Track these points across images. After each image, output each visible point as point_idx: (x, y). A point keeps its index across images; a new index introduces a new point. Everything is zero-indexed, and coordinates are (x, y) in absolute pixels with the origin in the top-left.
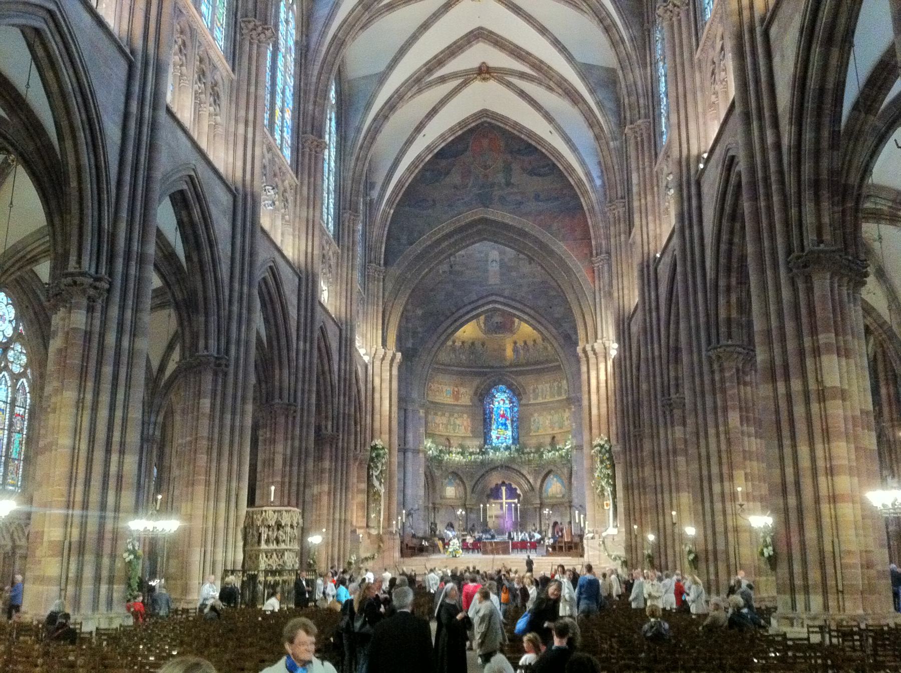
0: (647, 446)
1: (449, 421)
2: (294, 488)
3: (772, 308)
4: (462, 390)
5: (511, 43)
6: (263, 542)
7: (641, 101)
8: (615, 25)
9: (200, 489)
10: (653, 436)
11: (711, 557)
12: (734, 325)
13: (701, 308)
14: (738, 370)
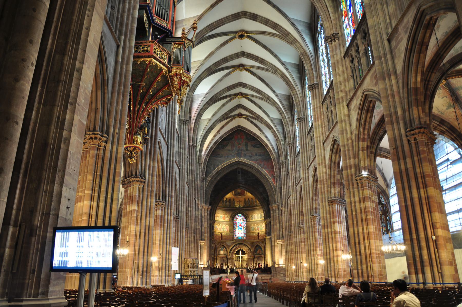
0: (293, 240)
1: (221, 227)
2: (188, 252)
3: (324, 211)
4: (226, 216)
6: (189, 268)
7: (291, 136)
8: (283, 113)
10: (295, 237)
11: (311, 271)
12: (317, 209)
13: (309, 204)
14: (318, 221)
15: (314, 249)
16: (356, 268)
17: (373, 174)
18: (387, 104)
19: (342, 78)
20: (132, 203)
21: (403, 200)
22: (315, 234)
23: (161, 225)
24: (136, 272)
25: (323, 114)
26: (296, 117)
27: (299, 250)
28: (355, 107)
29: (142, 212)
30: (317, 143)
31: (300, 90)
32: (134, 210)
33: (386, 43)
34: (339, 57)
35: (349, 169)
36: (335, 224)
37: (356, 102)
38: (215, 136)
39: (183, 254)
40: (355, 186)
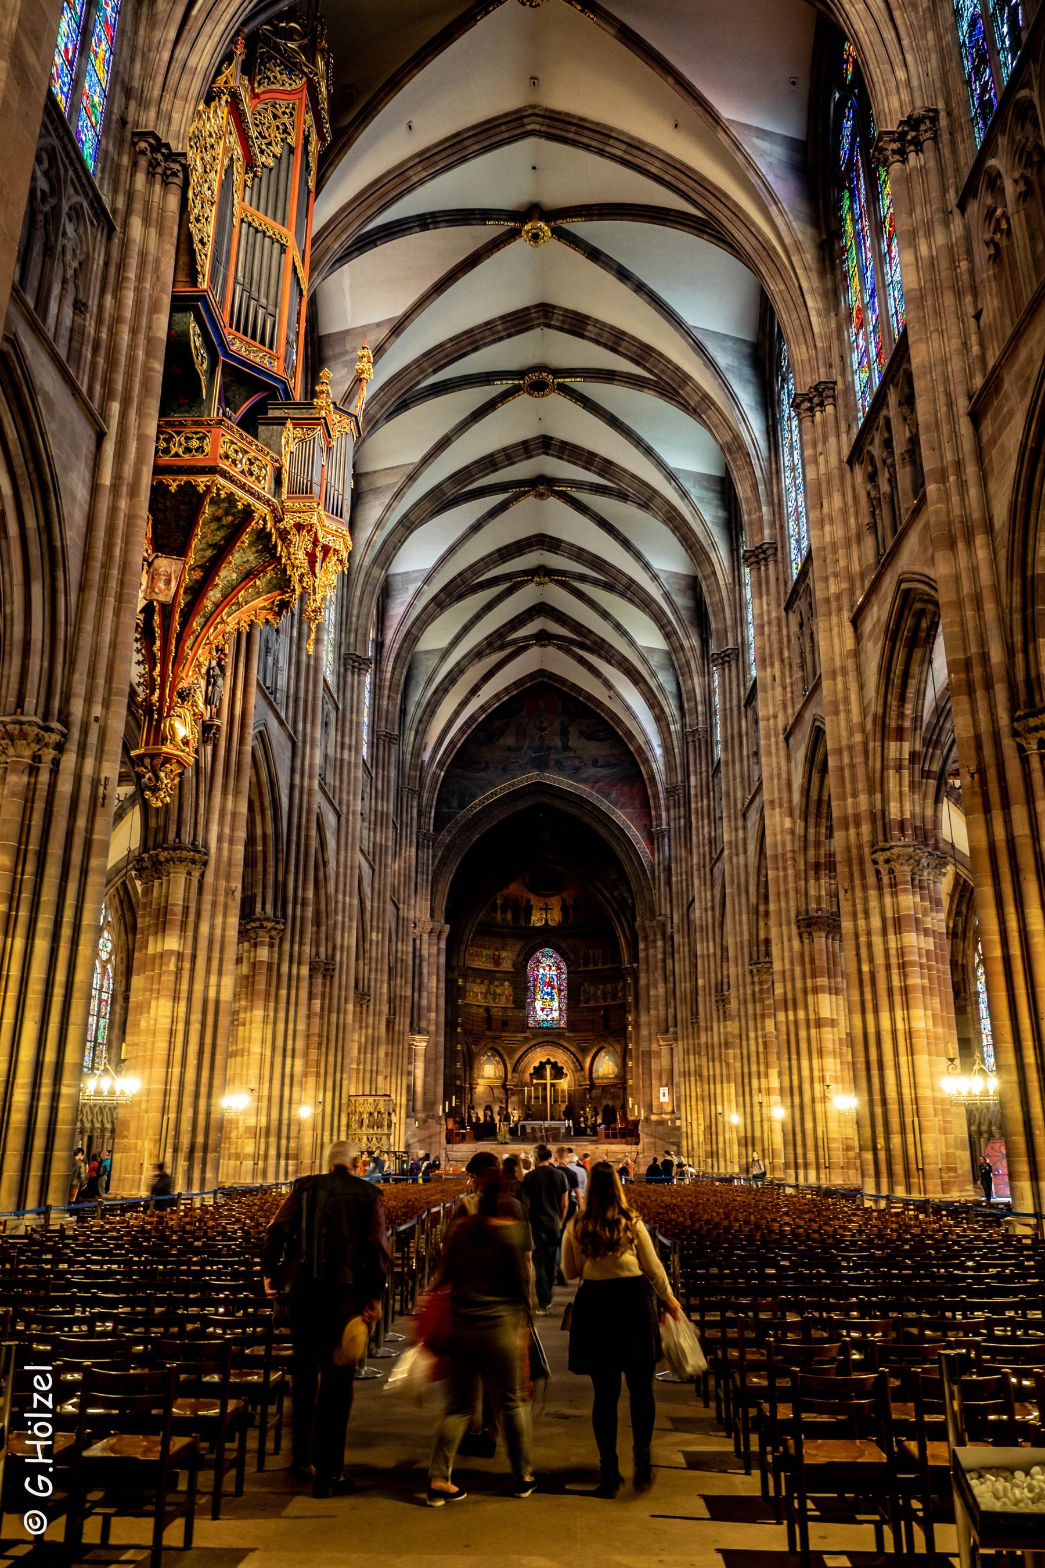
0: (703, 1040)
2: (368, 1075)
3: (786, 954)
4: (504, 954)
5: (573, 620)
7: (700, 708)
8: (676, 633)
9: (311, 1081)
10: (709, 1029)
13: (745, 927)
15: (759, 1072)
16: (870, 1143)
17: (932, 842)
18: (956, 629)
19: (840, 533)
20: (164, 930)
21: (996, 938)
22: (763, 1023)
23: (267, 993)
24: (170, 1150)
25: (789, 641)
26: (713, 649)
27: (718, 1072)
28: (873, 629)
29: (194, 957)
30: (768, 737)
31: (726, 563)
32: (171, 952)
33: (965, 427)
34: (834, 461)
35: (852, 825)
36: (820, 996)
37: (878, 614)
38: (464, 704)
39: (345, 1083)
40: (871, 880)
